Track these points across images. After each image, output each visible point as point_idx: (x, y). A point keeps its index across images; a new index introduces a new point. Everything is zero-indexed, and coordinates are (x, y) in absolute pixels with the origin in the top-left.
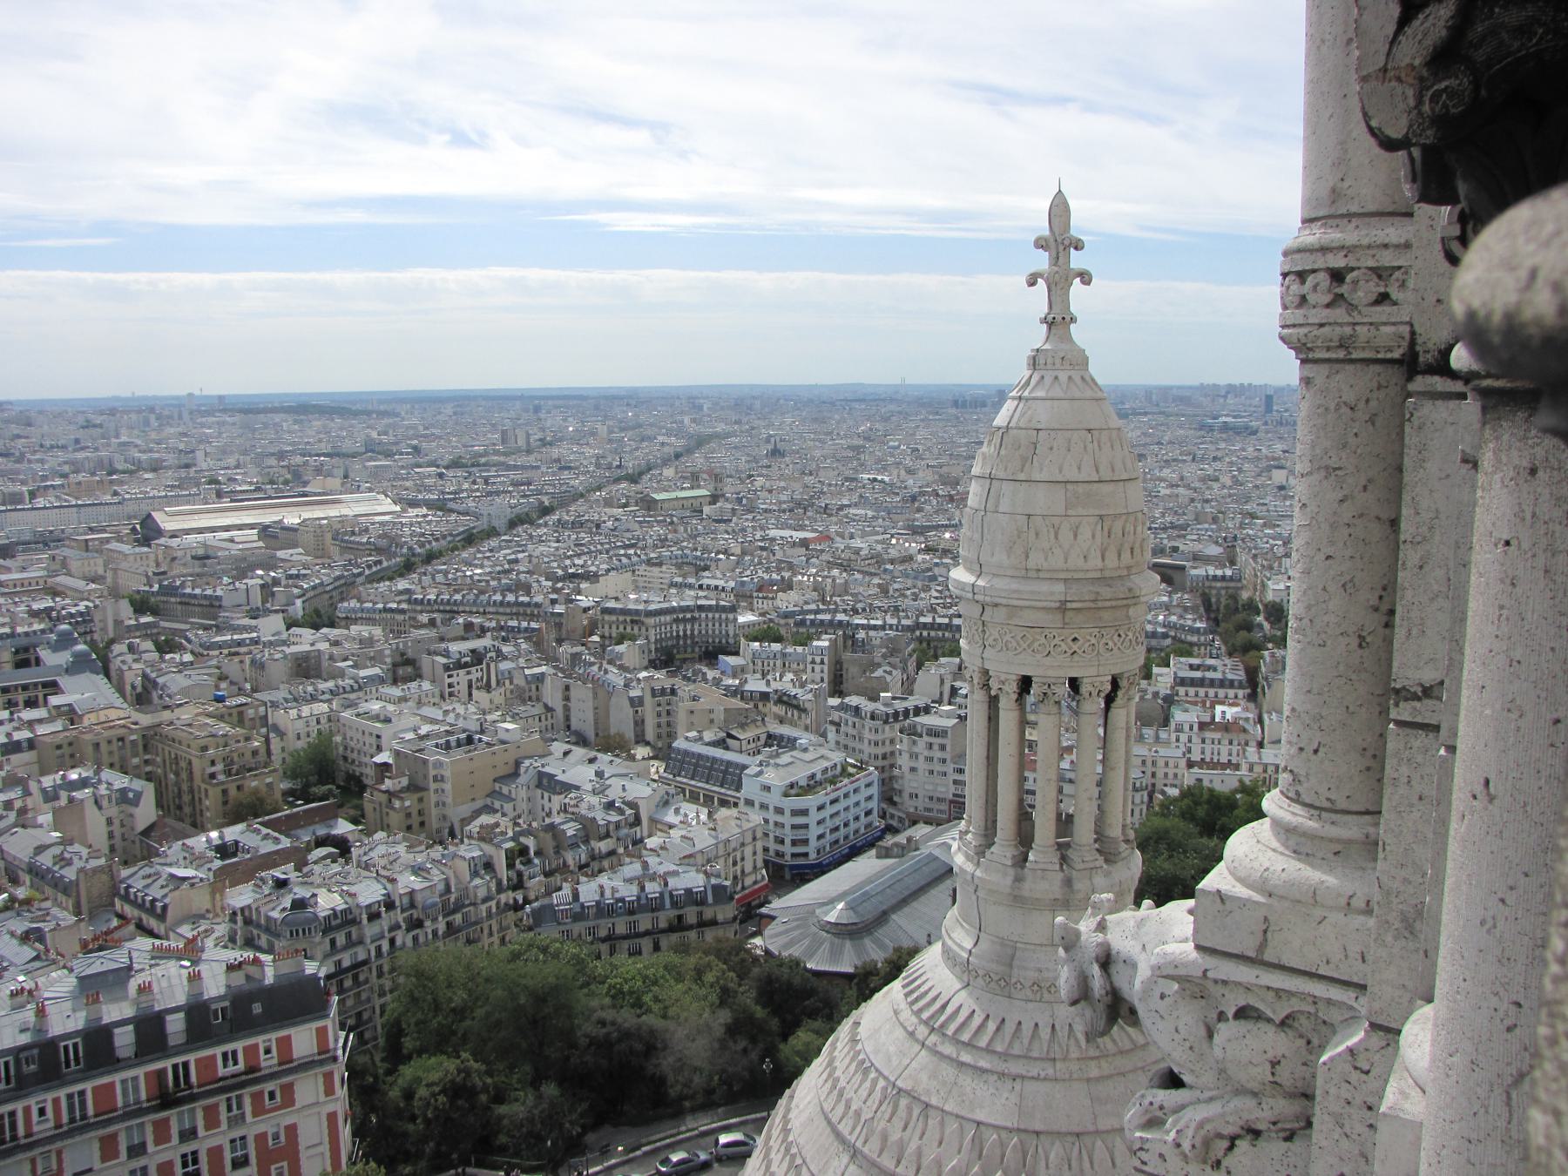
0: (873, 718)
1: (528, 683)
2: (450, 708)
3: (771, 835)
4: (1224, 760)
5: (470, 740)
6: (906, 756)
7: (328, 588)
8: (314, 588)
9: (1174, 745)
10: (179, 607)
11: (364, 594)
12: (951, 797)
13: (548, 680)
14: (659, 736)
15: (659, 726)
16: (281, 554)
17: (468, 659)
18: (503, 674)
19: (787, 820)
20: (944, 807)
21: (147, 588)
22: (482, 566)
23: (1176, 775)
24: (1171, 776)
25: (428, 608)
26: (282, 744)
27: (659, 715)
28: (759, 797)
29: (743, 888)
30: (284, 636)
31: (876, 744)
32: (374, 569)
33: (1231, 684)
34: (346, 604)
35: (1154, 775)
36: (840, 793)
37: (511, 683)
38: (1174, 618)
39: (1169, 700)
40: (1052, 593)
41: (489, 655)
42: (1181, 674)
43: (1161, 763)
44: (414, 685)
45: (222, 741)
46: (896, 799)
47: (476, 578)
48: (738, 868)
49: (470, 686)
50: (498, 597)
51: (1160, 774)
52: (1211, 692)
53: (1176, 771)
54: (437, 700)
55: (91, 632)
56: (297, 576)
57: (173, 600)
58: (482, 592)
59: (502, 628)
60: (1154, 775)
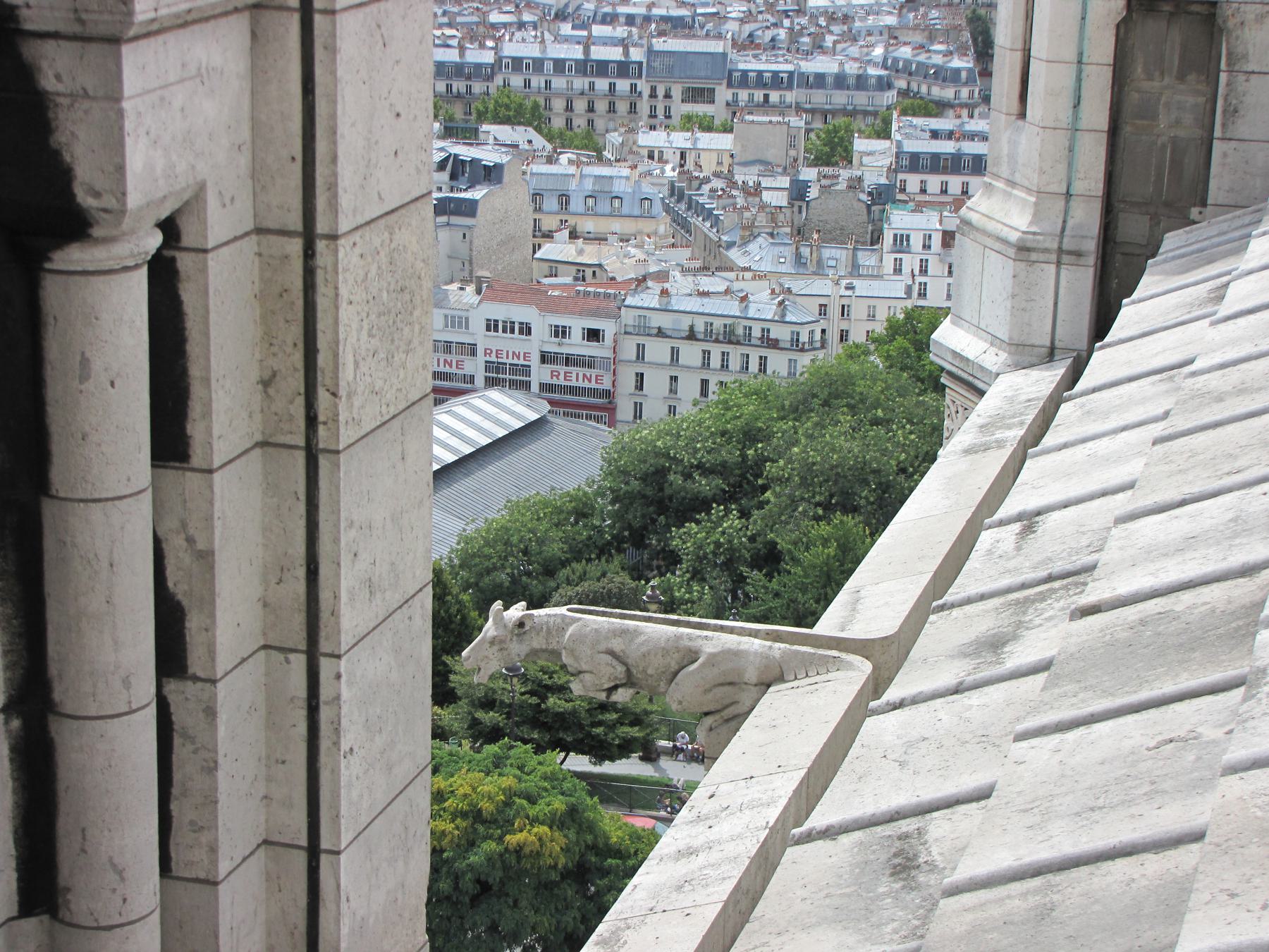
38: (905, 52)
39: (883, 196)
42: (910, 146)
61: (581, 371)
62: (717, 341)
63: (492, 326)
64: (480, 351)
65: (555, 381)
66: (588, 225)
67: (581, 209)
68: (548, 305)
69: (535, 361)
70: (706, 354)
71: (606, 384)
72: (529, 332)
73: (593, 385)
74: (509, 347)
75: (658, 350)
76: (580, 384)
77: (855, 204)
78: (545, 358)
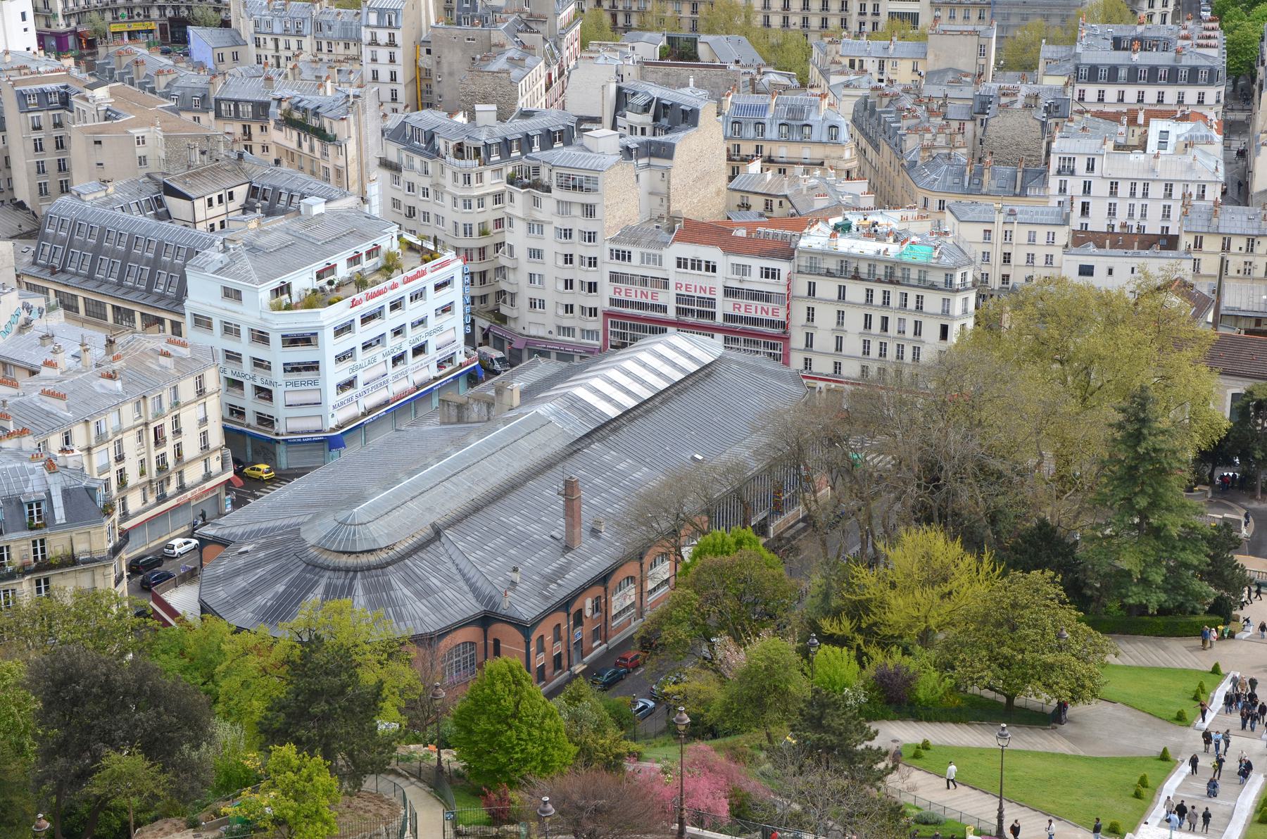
0: (460, 150)
3: (248, 385)
4: (1153, 227)
6: (520, 228)
9: (1053, 202)
12: (606, 305)
14: (43, 191)
15: (41, 168)
19: (278, 355)
20: (595, 324)
23: (1049, 259)
24: (1039, 260)
27: (38, 146)
28: (219, 309)
29: (182, 488)
31: (468, 204)
33: (1193, 76)
35: (1007, 258)
36: (385, 300)
42: (1089, 58)
43: (1020, 234)
46: (504, 310)
48: (169, 450)
51: (1019, 257)
52: (1151, 93)
53: (1050, 251)
60: (1007, 258)
61: (759, 304)
62: (879, 281)
63: (681, 263)
64: (672, 285)
65: (737, 313)
66: (781, 151)
67: (775, 135)
68: (731, 246)
69: (719, 295)
70: (870, 294)
71: (781, 317)
72: (714, 270)
73: (770, 317)
74: (696, 282)
75: (826, 288)
76: (759, 315)
77: (1031, 121)
78: (729, 292)
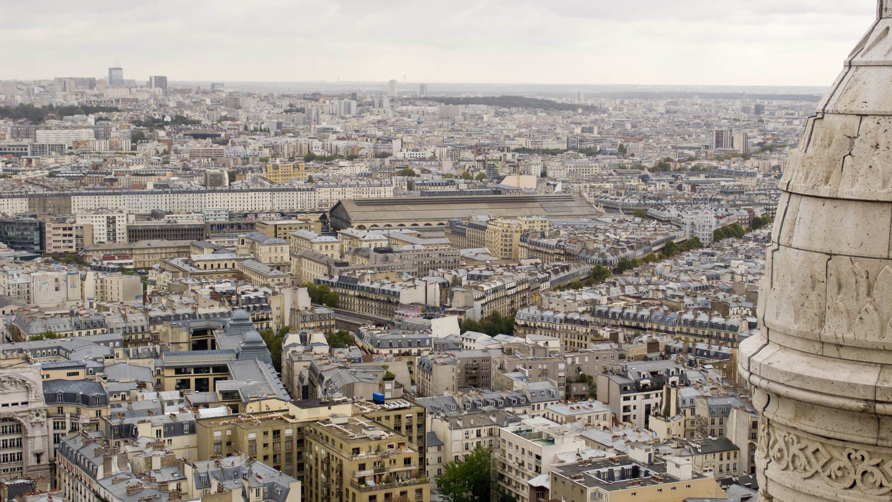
1: (712, 413)
2: (621, 433)
5: (635, 472)
7: (510, 292)
8: (495, 291)
10: (357, 301)
11: (546, 301)
13: (734, 413)
16: (465, 252)
17: (647, 382)
18: (684, 401)
21: (327, 279)
22: (677, 280)
25: (613, 322)
26: (440, 454)
30: (459, 340)
32: (562, 275)
34: (525, 310)
37: (693, 413)
40: (852, 386)
41: (671, 379)
44: (584, 404)
45: (374, 444)
47: (669, 292)
49: (648, 412)
50: (689, 316)
54: (607, 424)
55: (268, 319)
56: (479, 277)
57: (351, 293)
58: (673, 309)
59: (690, 350)
